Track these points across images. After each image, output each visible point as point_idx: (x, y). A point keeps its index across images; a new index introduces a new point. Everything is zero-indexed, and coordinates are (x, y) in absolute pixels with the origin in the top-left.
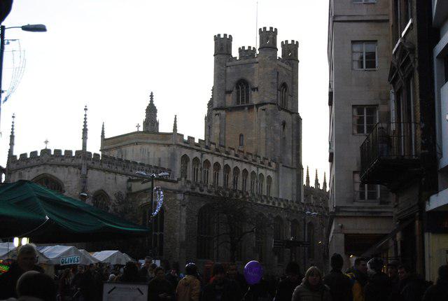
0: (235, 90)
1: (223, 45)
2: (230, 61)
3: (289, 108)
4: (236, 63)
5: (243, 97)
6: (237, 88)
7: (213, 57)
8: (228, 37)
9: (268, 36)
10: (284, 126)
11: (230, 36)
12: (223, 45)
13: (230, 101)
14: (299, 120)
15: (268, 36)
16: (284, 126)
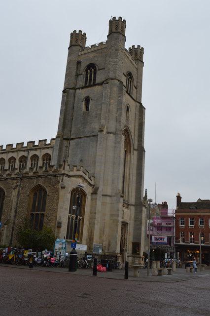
0: (84, 73)
1: (77, 39)
2: (82, 51)
3: (134, 96)
4: (89, 51)
5: (90, 81)
6: (87, 72)
7: (67, 51)
8: (82, 34)
9: (117, 27)
10: (128, 110)
11: (85, 34)
12: (77, 39)
13: (81, 83)
14: (142, 109)
15: (117, 27)
16: (128, 110)
